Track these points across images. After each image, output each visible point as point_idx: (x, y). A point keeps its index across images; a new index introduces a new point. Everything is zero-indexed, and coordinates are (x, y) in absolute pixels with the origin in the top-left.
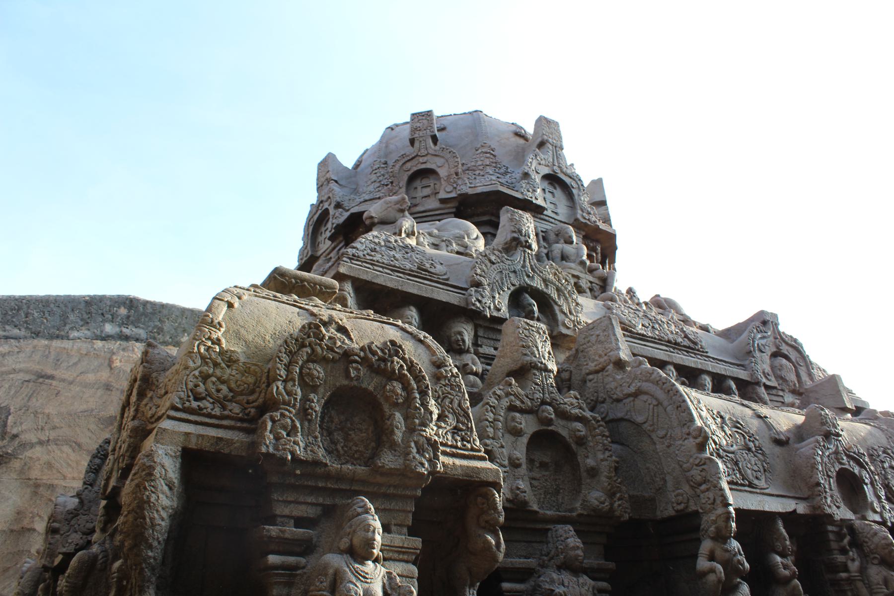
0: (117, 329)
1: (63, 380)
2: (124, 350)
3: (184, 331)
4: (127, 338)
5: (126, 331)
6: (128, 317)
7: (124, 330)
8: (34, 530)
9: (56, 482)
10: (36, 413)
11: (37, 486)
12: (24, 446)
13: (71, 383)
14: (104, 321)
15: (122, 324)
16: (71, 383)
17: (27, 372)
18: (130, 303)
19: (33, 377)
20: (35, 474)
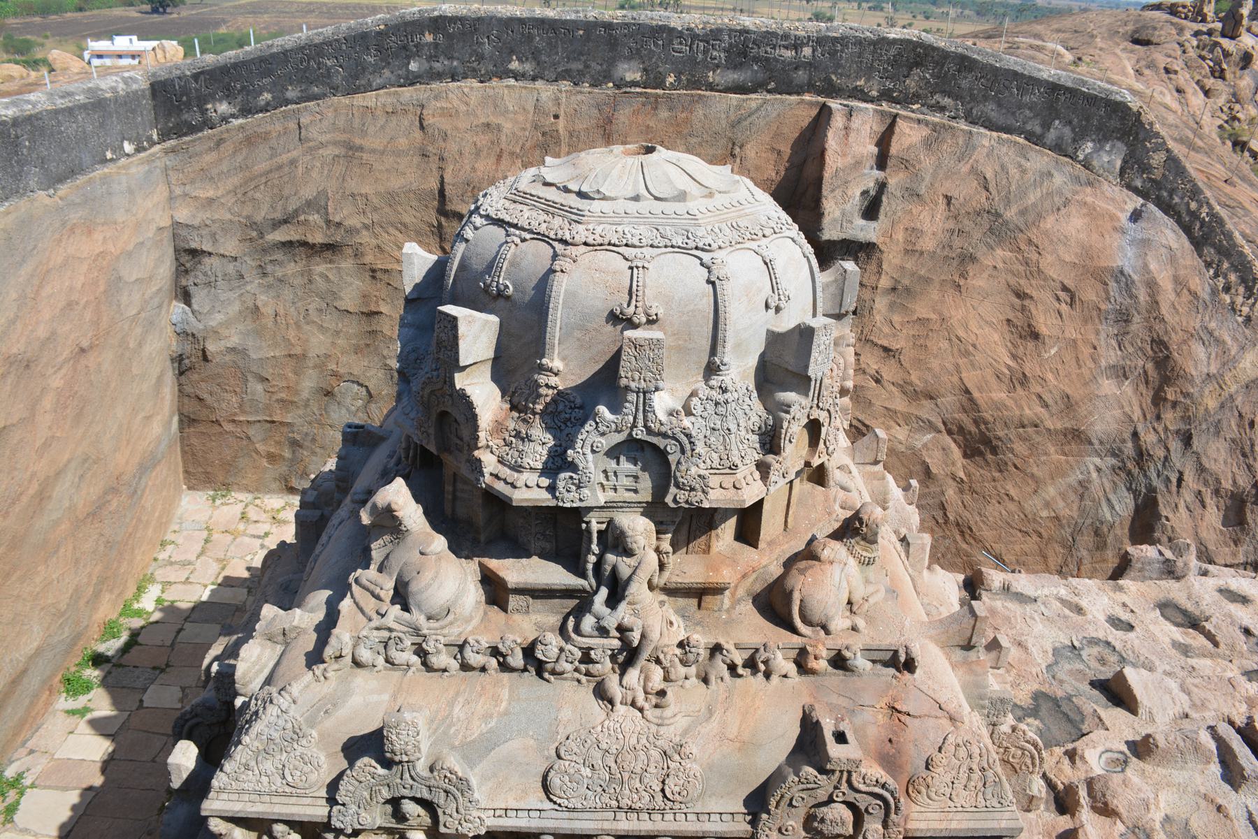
0: (426, 66)
1: (373, 151)
2: (436, 98)
3: (512, 52)
4: (439, 76)
5: (437, 66)
6: (436, 45)
7: (437, 66)
8: (379, 313)
9: (389, 267)
10: (353, 195)
11: (373, 271)
12: (351, 231)
13: (382, 153)
14: (409, 58)
15: (430, 58)
16: (382, 153)
17: (335, 143)
18: (438, 24)
19: (343, 151)
20: (368, 259)
